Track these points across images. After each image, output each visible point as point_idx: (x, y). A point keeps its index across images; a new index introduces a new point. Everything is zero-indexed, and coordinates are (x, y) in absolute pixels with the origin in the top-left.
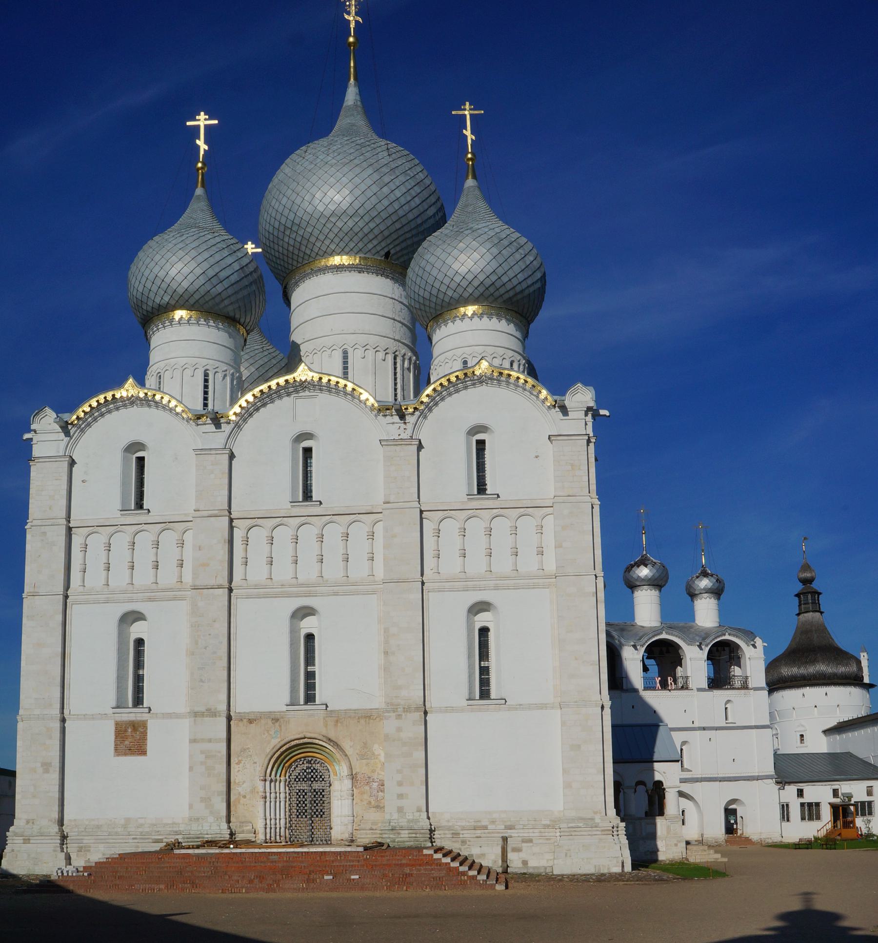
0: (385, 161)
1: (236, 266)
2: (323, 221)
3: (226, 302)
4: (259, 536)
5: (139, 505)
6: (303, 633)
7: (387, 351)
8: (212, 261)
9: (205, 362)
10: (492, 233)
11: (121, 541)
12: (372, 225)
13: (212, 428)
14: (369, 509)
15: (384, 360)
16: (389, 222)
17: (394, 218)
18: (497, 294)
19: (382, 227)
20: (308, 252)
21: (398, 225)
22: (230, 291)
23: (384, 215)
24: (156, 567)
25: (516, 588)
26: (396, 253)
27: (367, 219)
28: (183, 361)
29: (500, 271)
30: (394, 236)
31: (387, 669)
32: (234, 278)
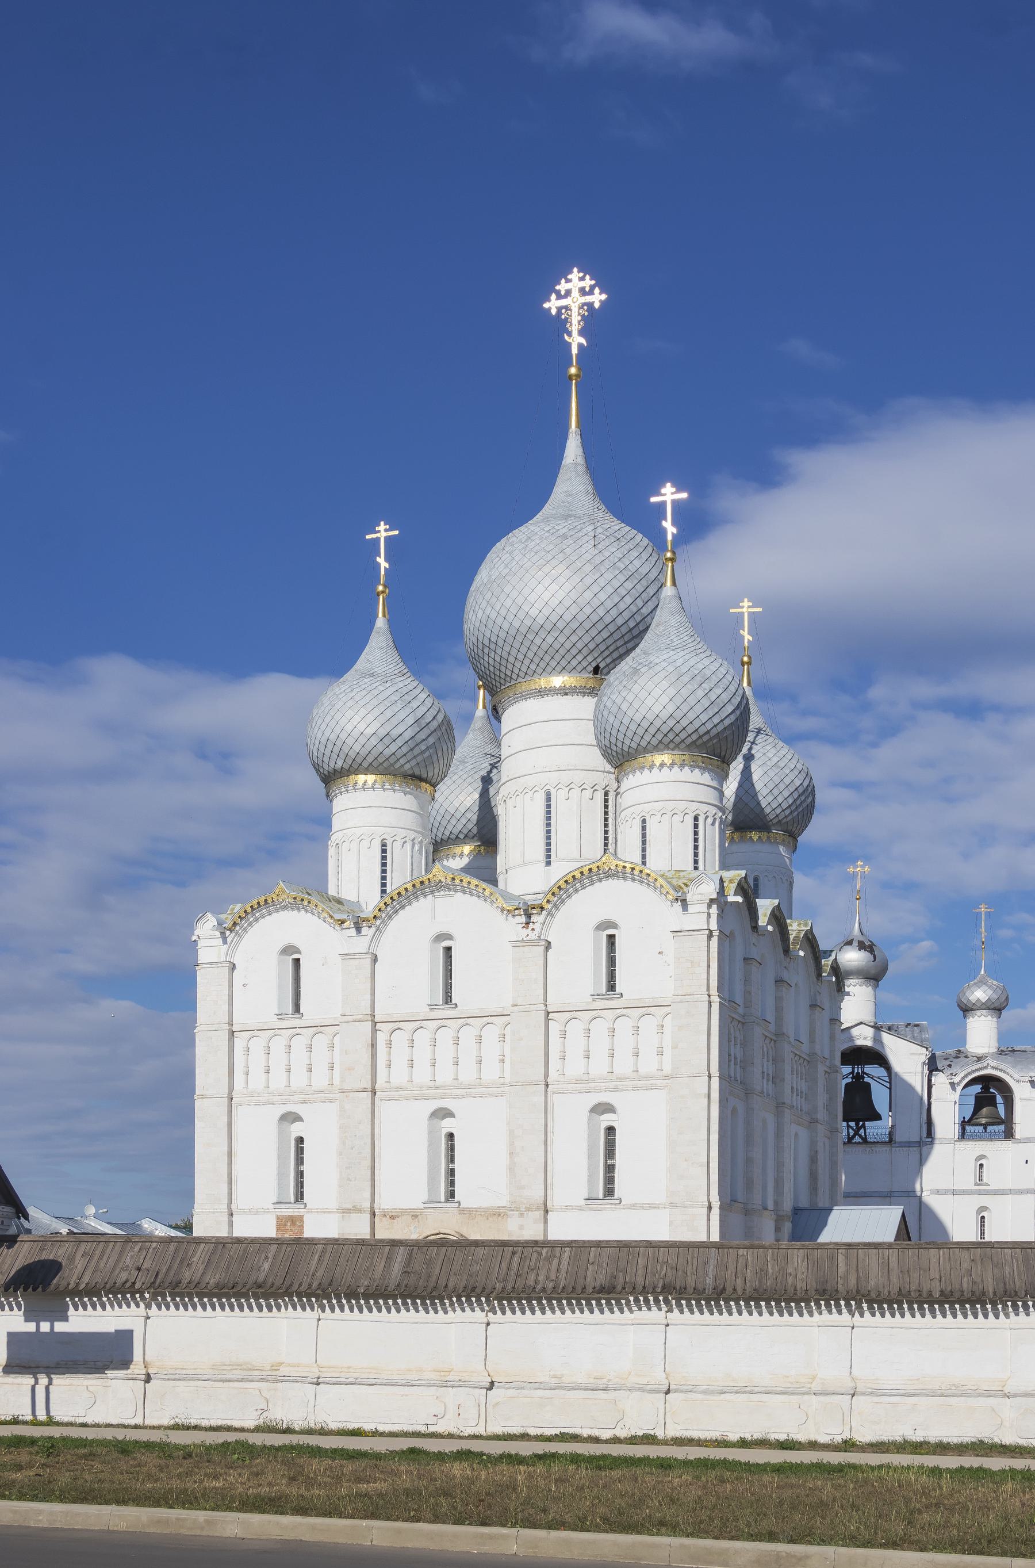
0: (588, 556)
1: (411, 720)
2: (519, 638)
3: (402, 761)
4: (400, 1039)
5: (297, 1009)
6: (444, 1132)
7: (595, 788)
8: (383, 719)
9: (382, 830)
10: (670, 669)
11: (278, 1044)
12: (574, 638)
13: (353, 931)
14: (499, 1011)
15: (592, 799)
16: (594, 632)
17: (600, 626)
18: (677, 740)
19: (586, 639)
20: (509, 673)
21: (605, 634)
22: (405, 749)
23: (587, 625)
24: (310, 1070)
25: (635, 1089)
26: (604, 668)
27: (567, 632)
28: (359, 832)
29: (678, 715)
30: (602, 647)
31: (511, 1169)
32: (407, 735)
